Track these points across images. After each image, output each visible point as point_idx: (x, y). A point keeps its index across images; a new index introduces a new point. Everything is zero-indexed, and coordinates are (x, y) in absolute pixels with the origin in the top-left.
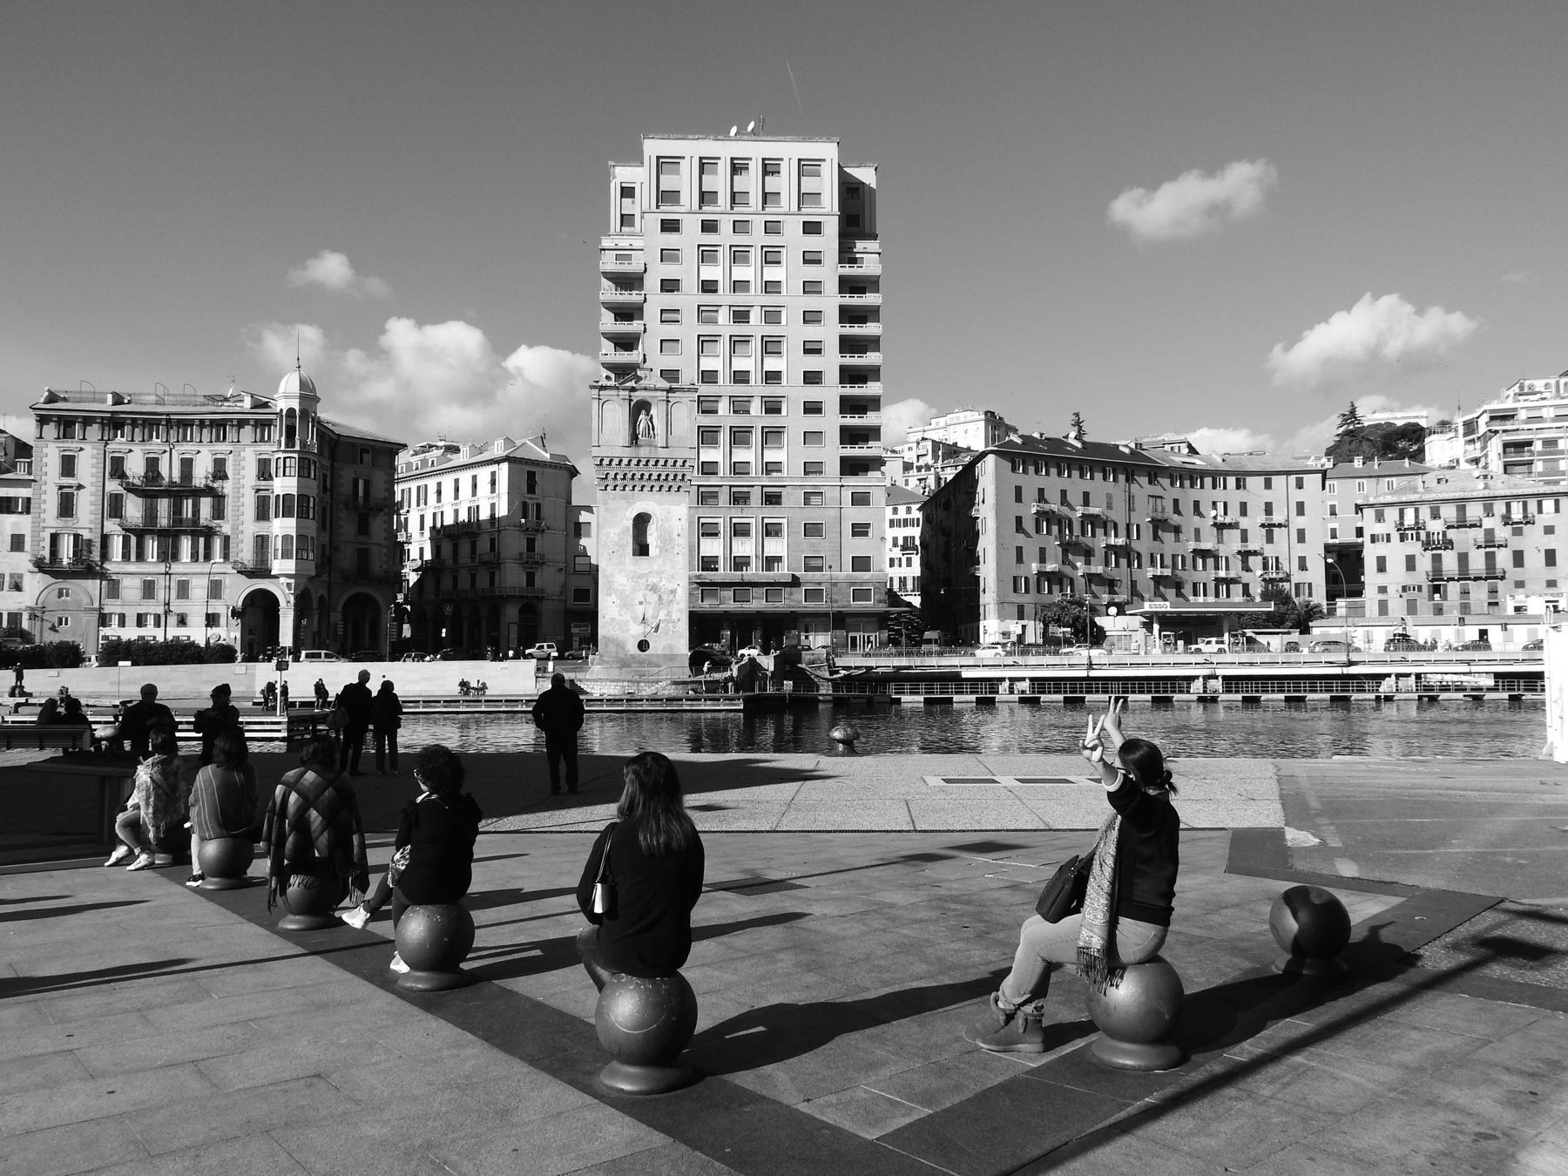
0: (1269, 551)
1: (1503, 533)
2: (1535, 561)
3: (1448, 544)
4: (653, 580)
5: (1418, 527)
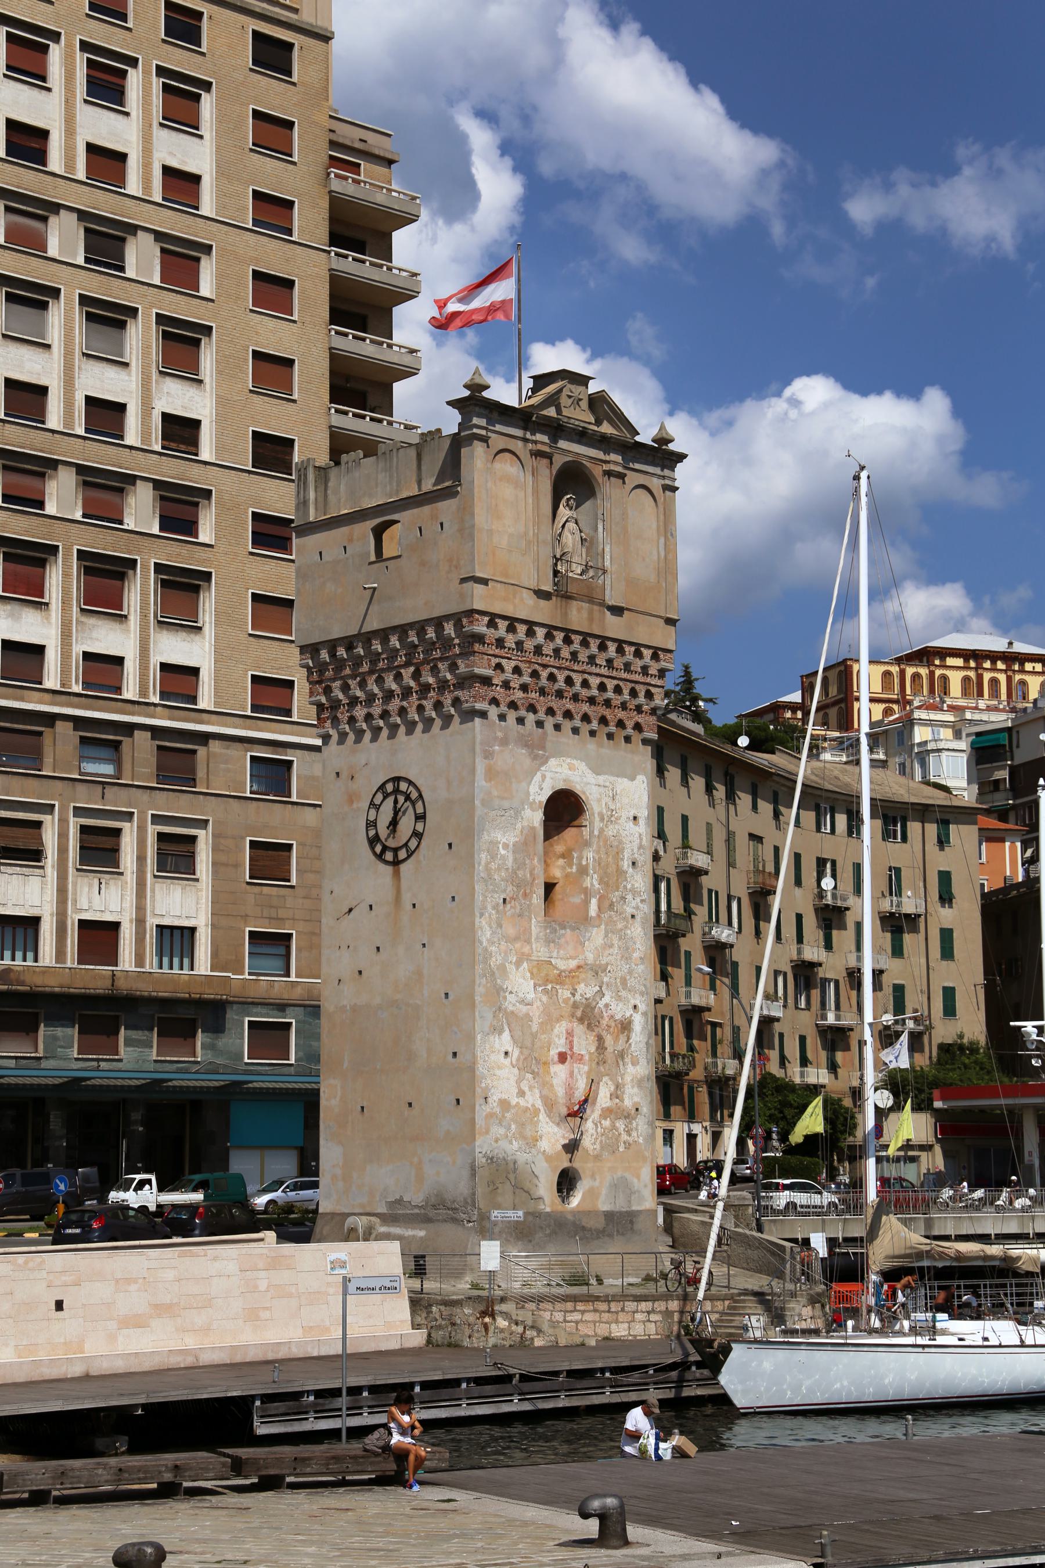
4: (586, 990)
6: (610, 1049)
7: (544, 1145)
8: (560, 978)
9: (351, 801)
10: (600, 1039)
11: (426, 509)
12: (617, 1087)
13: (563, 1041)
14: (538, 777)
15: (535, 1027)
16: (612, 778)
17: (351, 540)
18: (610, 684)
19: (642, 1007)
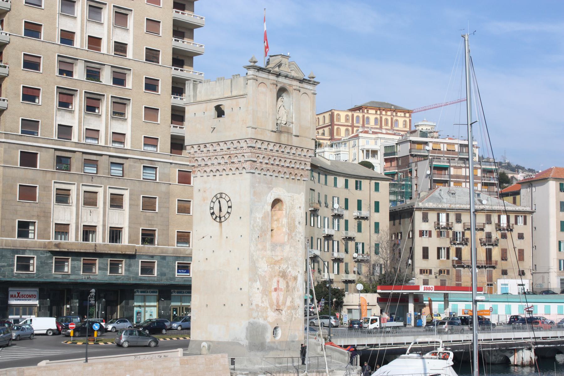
0: (359, 238)
1: (496, 235)
2: (512, 256)
3: (465, 242)
4: (284, 266)
5: (449, 227)
6: (291, 286)
7: (270, 319)
8: (276, 262)
9: (204, 200)
10: (287, 283)
11: (234, 101)
12: (293, 299)
13: (276, 284)
14: (270, 194)
15: (267, 279)
16: (293, 194)
17: (206, 110)
18: (293, 161)
19: (301, 272)
